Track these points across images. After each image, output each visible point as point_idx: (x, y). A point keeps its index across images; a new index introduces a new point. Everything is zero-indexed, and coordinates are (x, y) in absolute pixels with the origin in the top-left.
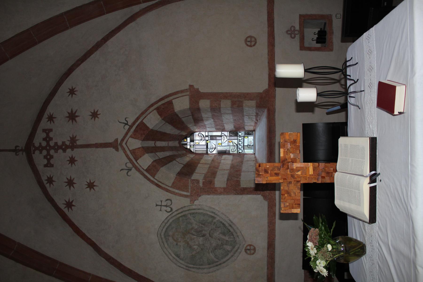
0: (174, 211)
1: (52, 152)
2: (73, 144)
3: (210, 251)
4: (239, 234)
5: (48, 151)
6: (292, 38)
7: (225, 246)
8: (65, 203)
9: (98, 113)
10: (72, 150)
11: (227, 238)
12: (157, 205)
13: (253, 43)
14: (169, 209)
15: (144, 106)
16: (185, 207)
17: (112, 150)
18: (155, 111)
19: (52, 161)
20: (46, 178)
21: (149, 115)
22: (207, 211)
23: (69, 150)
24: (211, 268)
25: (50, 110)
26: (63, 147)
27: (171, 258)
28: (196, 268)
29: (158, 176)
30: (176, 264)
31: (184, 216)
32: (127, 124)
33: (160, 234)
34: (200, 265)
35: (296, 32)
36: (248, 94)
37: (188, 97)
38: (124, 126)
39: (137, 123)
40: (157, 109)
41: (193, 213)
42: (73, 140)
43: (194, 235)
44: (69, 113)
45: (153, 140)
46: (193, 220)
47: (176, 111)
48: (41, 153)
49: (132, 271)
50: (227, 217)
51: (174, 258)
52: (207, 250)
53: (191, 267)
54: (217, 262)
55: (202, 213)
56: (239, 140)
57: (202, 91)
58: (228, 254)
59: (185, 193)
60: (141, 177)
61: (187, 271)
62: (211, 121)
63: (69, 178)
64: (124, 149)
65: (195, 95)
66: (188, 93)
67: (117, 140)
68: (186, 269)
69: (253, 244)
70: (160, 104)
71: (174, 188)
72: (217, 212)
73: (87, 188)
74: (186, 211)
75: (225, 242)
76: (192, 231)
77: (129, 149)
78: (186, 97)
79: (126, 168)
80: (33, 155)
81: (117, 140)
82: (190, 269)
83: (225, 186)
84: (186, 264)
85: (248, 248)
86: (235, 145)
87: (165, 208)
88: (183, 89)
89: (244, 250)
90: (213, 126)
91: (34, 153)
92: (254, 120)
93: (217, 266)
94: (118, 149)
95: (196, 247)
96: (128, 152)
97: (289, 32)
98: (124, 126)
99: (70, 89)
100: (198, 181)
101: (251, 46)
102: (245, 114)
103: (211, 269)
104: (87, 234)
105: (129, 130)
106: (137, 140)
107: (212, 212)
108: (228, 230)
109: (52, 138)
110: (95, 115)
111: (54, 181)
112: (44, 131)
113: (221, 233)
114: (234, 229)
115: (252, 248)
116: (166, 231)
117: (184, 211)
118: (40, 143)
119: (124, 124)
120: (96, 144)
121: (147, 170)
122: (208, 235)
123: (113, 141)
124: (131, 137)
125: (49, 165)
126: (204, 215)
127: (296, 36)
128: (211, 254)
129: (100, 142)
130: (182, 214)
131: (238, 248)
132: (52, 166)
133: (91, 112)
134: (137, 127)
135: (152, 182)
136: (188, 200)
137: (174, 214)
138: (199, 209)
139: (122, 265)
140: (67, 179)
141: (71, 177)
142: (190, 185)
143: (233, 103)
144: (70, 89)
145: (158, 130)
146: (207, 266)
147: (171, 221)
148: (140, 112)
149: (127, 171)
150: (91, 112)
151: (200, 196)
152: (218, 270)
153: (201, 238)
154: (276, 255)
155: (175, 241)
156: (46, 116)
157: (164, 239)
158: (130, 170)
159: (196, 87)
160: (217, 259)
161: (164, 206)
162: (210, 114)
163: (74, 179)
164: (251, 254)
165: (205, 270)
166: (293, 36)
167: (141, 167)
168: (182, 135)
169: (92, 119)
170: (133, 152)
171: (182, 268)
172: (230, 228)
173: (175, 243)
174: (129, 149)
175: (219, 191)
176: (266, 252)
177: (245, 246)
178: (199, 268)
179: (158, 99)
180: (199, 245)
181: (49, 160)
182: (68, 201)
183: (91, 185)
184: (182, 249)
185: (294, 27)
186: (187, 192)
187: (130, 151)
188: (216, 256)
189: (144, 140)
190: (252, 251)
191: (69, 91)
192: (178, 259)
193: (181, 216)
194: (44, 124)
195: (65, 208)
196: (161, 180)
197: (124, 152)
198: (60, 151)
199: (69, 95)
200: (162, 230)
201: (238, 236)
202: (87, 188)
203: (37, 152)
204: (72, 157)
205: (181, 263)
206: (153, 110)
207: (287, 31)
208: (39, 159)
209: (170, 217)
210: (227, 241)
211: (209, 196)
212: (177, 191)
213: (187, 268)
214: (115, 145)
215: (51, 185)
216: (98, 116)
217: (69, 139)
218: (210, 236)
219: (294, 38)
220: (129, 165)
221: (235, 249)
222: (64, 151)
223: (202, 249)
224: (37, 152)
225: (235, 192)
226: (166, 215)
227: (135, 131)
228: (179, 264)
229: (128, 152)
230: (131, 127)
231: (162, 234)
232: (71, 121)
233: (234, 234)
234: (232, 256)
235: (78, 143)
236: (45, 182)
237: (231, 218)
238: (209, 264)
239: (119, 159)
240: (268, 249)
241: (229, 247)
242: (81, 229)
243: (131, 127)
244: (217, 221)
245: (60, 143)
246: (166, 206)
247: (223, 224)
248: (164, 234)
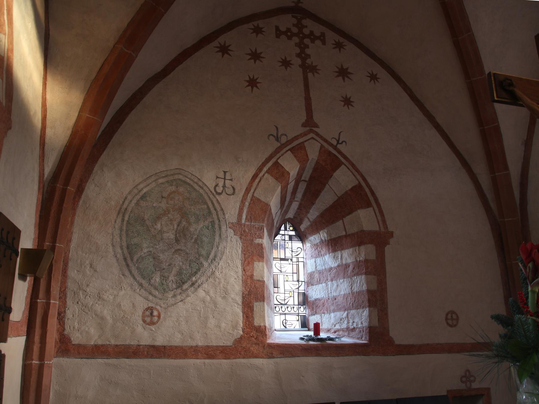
0: (217, 197)
1: (296, 39)
2: (308, 69)
3: (151, 249)
4: (179, 297)
5: (296, 35)
6: (461, 378)
7: (158, 274)
8: (227, 45)
9: (350, 106)
10: (300, 66)
11: (171, 278)
12: (225, 172)
13: (450, 322)
14: (219, 189)
16: (224, 214)
17: (303, 118)
18: (356, 183)
19: (283, 37)
20: (261, 26)
21: (351, 173)
22: (218, 247)
23: (299, 61)
24: (122, 248)
25: (349, 47)
26: (303, 55)
27: (141, 186)
28: (122, 224)
29: (269, 180)
30: (130, 193)
31: (210, 213)
32: (338, 143)
33: (180, 174)
34: (127, 231)
35: (468, 383)
36: (386, 314)
37: (378, 229)
38: (335, 139)
39: (339, 156)
40: (359, 186)
41: (213, 226)
42: (314, 69)
43: (178, 225)
44: (347, 69)
45: (311, 177)
46: (202, 226)
47: (359, 211)
48: (294, 25)
49: (121, 124)
50: (207, 280)
51: (140, 191)
52: (152, 245)
53: (124, 216)
54: (132, 260)
55: (214, 239)
56: (294, 308)
57: (386, 248)
58: (144, 278)
59: (244, 217)
60: (267, 155)
61: (118, 209)
63: (262, 55)
64: (305, 134)
65: (379, 239)
66: (382, 229)
67: (317, 126)
68: (120, 209)
69: (161, 320)
70: (367, 190)
71: (251, 200)
72: (215, 263)
73: (250, 77)
74: (217, 215)
75: (166, 274)
76: (184, 223)
77: (306, 141)
78: (378, 226)
79: (279, 135)
80: (291, 15)
81: (317, 126)
82: (121, 215)
83: (255, 278)
84: (130, 209)
85: (155, 313)
86: (286, 301)
87: (221, 184)
88: (387, 223)
89: (150, 305)
90: (319, 268)
91: (293, 16)
92: (338, 327)
93: (125, 259)
94: (305, 127)
95: (159, 226)
96: (301, 140)
97: (468, 373)
98: (335, 139)
99: (376, 75)
100: (261, 237)
101: (447, 319)
102: (353, 312)
103: (119, 250)
104: (181, 67)
105: (331, 145)
106: (318, 153)
107: (215, 256)
108: (185, 281)
109: (314, 43)
110: (347, 102)
111: (257, 36)
112: (323, 34)
113: (181, 269)
114: (187, 289)
115: (156, 319)
116: (185, 182)
117: (217, 212)
118: (306, 27)
119: (337, 139)
120: (310, 98)
122: (179, 247)
123: (315, 121)
124: (322, 146)
125: (279, 33)
126: (211, 243)
127: (464, 385)
128: (145, 251)
129: (313, 104)
130: (212, 209)
131: (155, 297)
132: (278, 36)
133: (350, 97)
134: (335, 155)
135: (260, 169)
136: (234, 220)
137: (211, 196)
138: (220, 235)
139: (131, 111)
140: (261, 53)
141: (264, 58)
142: (257, 225)
144: (376, 75)
145: (327, 186)
146: (124, 244)
147: (201, 191)
148: (354, 163)
149: (275, 135)
150: (350, 97)
151: (241, 238)
152: (117, 260)
153: (172, 237)
154: (142, 360)
155: (169, 195)
156: (342, 40)
157: (171, 178)
158: (277, 139)
159: (391, 241)
160: (137, 260)
161: (224, 182)
163: (261, 61)
164: (144, 316)
165: (119, 240)
166: (464, 379)
167: (282, 155)
168: (301, 223)
169: (342, 97)
171: (123, 202)
172: (190, 283)
173: (165, 195)
174: (306, 141)
175: (248, 268)
176: (147, 344)
177: (158, 307)
178: (121, 230)
179: (373, 188)
180: (161, 232)
181: (285, 33)
182: (230, 48)
184: (154, 205)
185: (474, 381)
186: (246, 219)
187: (303, 143)
188: (142, 258)
190: (148, 320)
191: (375, 73)
192: (138, 197)
193: (208, 208)
194: (331, 37)
195: (220, 43)
196: (262, 182)
197: (301, 134)
198: (298, 50)
199: (369, 73)
200: (186, 177)
201: (174, 296)
202: (250, 77)
203: (295, 21)
204: (291, 64)
205: (131, 201)
206: (358, 180)
207: (468, 371)
208: (286, 22)
209: (207, 190)
210: (168, 278)
211: (240, 251)
212: (247, 204)
213: (123, 210)
214: (310, 123)
215: (252, 31)
216: (346, 106)
217: (314, 64)
218: (177, 251)
219: (462, 381)
220: (284, 140)
221: (153, 291)
222: (298, 55)
223: (154, 236)
224: (295, 21)
225: (247, 293)
226: (211, 184)
227: (330, 153)
228: (129, 198)
229: (301, 140)
231: (181, 177)
232: (337, 70)
233: (179, 291)
234: (141, 285)
235: (310, 75)
236: (255, 23)
237: (205, 286)
238: (128, 248)
240: (153, 347)
241: (158, 280)
242: (189, 59)
243: (335, 148)
244: (201, 263)
245: (308, 51)
246: (224, 186)
247: (196, 273)
248: (180, 179)
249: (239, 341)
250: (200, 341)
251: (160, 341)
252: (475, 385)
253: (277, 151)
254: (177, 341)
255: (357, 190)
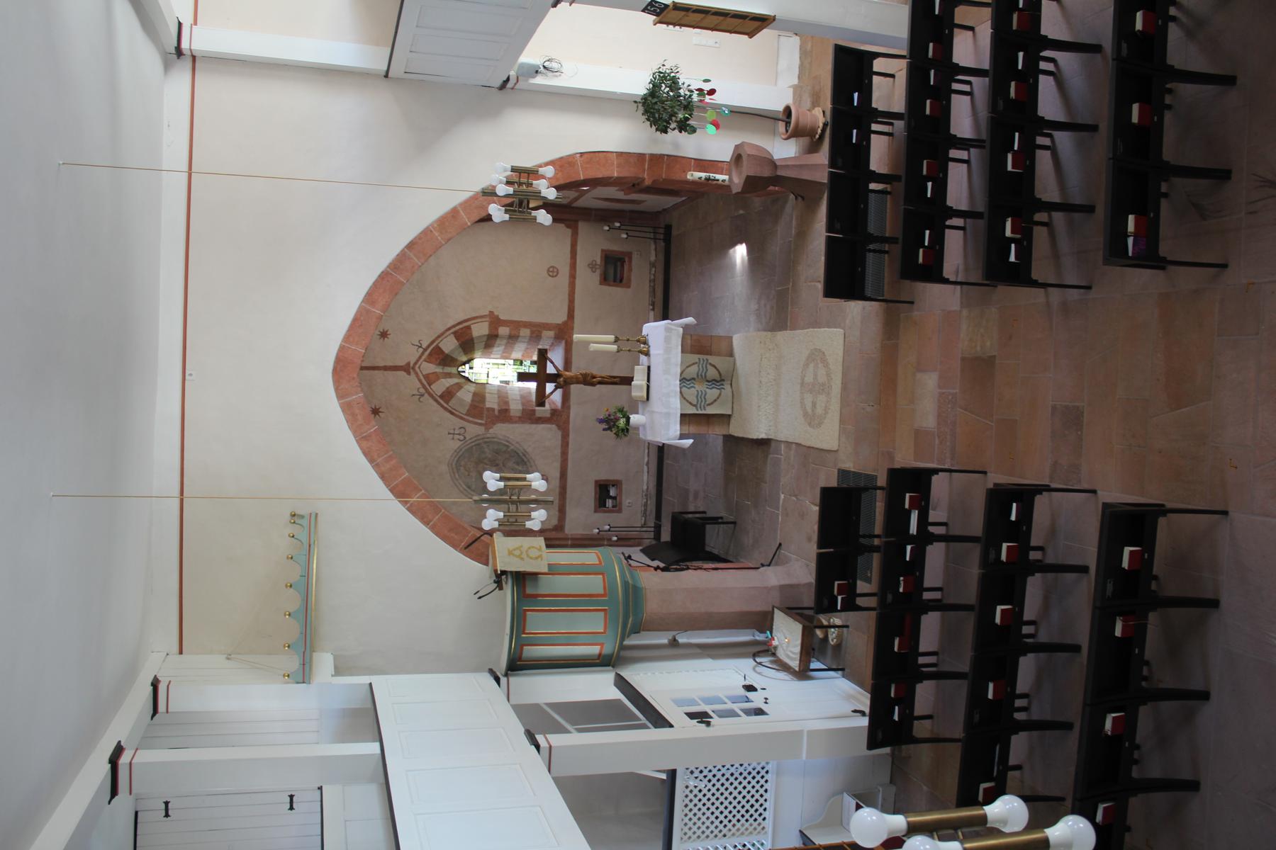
15: (442, 329)
17: (403, 373)
40: (455, 333)
62: (502, 348)
65: (495, 322)
81: (408, 364)
100: (493, 410)
110: (384, 335)
121: (442, 396)
135: (445, 409)
136: (483, 428)
143: (532, 332)
162: (504, 342)
170: (426, 377)
183: (376, 412)
189: (439, 364)
214: (407, 369)
220: (422, 390)
227: (430, 354)
230: (425, 350)
239: (411, 383)
243: (425, 350)
249: (559, 427)
250: (558, 451)
251: (558, 475)
252: (599, 261)
253: (431, 395)
254: (557, 465)
255: (457, 335)
